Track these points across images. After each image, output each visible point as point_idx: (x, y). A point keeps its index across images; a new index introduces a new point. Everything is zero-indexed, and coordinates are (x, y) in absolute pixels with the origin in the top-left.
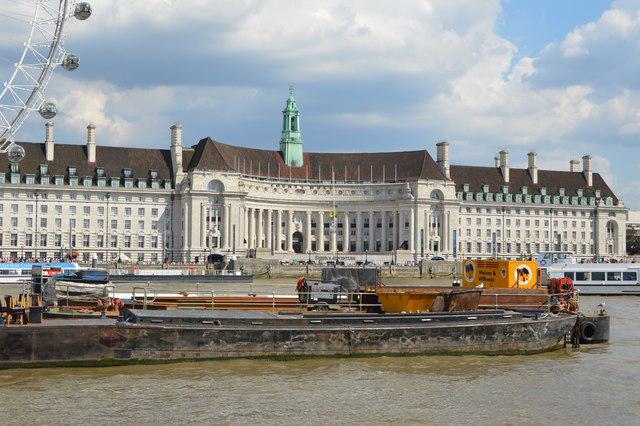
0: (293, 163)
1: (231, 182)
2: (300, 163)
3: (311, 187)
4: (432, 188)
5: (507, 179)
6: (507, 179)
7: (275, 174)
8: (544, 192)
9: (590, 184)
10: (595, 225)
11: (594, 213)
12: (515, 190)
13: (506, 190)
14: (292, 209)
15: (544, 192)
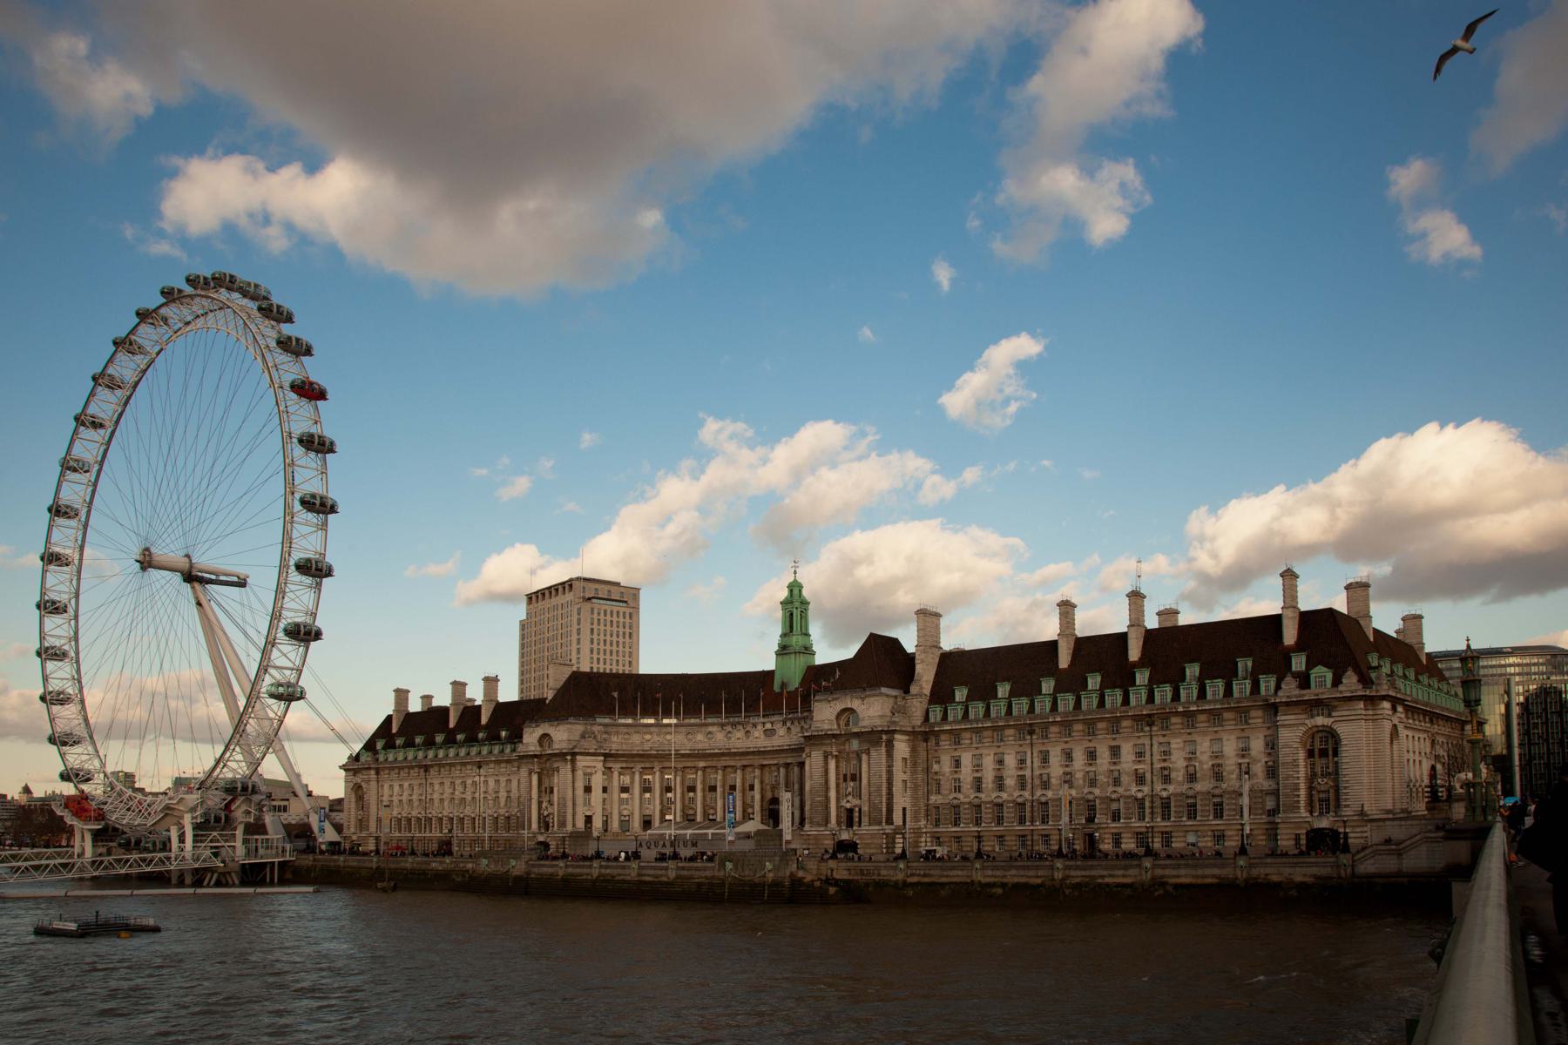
0: (783, 685)
1: (562, 735)
2: (795, 683)
3: (784, 723)
4: (839, 706)
5: (1064, 661)
6: (1064, 661)
7: (733, 709)
8: (1142, 677)
9: (1290, 636)
10: (1272, 745)
11: (1272, 709)
12: (1072, 682)
13: (1047, 686)
14: (758, 761)
15: (1142, 677)
